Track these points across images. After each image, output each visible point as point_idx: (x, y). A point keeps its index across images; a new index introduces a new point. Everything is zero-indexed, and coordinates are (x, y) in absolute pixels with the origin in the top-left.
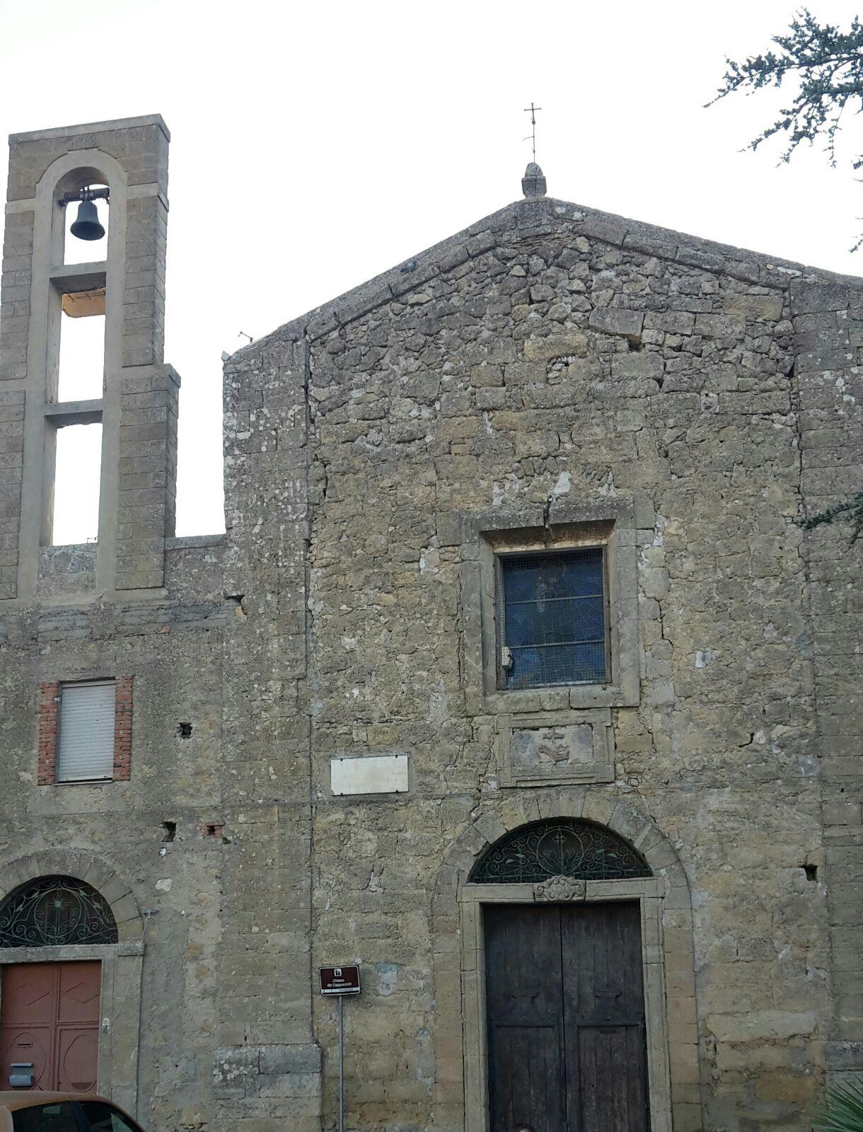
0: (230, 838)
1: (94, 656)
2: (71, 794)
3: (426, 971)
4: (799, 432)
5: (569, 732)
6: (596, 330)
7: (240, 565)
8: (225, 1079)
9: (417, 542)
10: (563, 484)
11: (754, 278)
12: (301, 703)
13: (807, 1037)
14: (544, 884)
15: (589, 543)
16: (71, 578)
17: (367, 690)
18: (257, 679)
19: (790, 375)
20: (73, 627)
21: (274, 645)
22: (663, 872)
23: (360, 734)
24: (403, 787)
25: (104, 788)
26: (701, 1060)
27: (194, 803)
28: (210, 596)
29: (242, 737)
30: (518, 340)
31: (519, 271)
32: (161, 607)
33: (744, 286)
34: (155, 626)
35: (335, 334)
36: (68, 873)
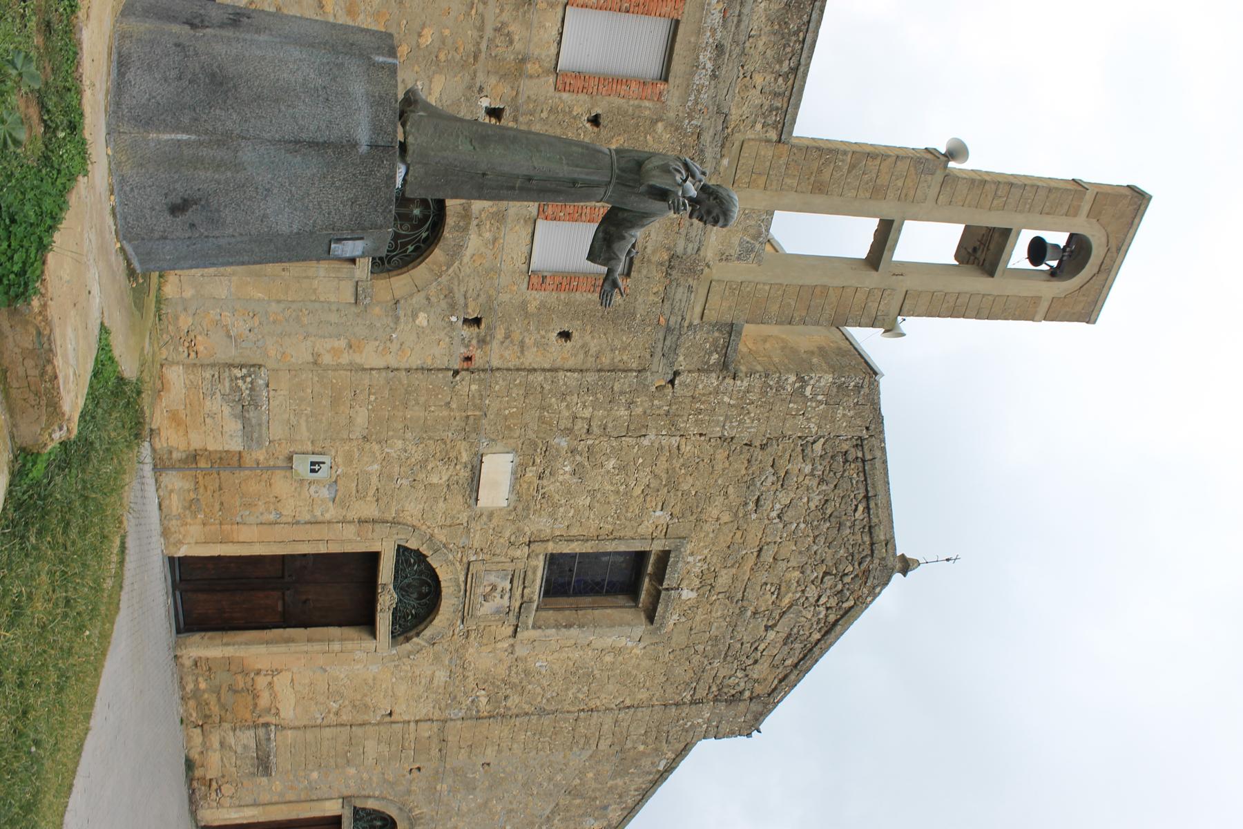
0: (458, 378)
2: (525, 233)
3: (328, 516)
6: (790, 607)
8: (237, 378)
9: (676, 511)
13: (277, 714)
17: (567, 476)
20: (688, 240)
23: (531, 473)
28: (681, 358)
34: (667, 312)
35: (860, 455)
36: (447, 233)
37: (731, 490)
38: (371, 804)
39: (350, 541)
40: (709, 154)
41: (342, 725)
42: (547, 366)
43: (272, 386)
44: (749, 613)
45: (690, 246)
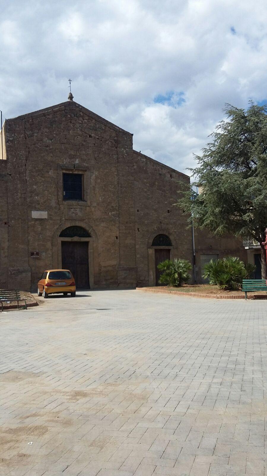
0: (10, 225)
3: (51, 253)
4: (118, 159)
5: (78, 210)
7: (11, 167)
10: (77, 162)
11: (111, 128)
12: (25, 199)
13: (115, 265)
17: (39, 197)
18: (15, 192)
19: (116, 148)
21: (19, 186)
23: (37, 206)
26: (99, 269)
28: (3, 173)
29: (12, 205)
30: (69, 130)
31: (69, 116)
33: (109, 129)
35: (31, 120)
38: (151, 241)
41: (120, 249)
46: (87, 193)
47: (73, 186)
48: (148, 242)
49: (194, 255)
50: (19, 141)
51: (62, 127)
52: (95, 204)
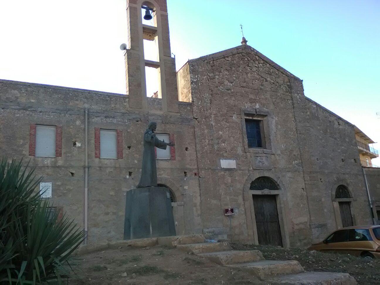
0: (201, 176)
1: (164, 128)
3: (243, 210)
5: (264, 158)
7: (197, 111)
12: (213, 145)
14: (264, 190)
15: (259, 119)
16: (156, 107)
21: (206, 131)
22: (283, 189)
23: (225, 155)
24: (235, 168)
25: (169, 162)
26: (292, 228)
27: (191, 167)
28: (189, 117)
30: (247, 74)
31: (246, 59)
32: (179, 118)
35: (212, 62)
36: (163, 183)
37: (225, 98)
38: (334, 193)
39: (250, 202)
40: (134, 117)
42: (195, 153)
43: (208, 227)
44: (262, 87)
45: (159, 119)
46: (270, 139)
47: (255, 132)
48: (332, 195)
49: (372, 207)
50: (203, 83)
51: (240, 70)
52: (279, 152)
